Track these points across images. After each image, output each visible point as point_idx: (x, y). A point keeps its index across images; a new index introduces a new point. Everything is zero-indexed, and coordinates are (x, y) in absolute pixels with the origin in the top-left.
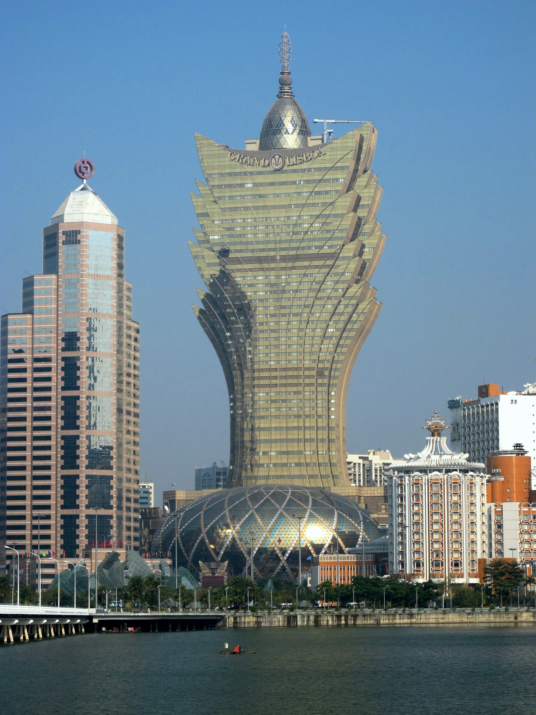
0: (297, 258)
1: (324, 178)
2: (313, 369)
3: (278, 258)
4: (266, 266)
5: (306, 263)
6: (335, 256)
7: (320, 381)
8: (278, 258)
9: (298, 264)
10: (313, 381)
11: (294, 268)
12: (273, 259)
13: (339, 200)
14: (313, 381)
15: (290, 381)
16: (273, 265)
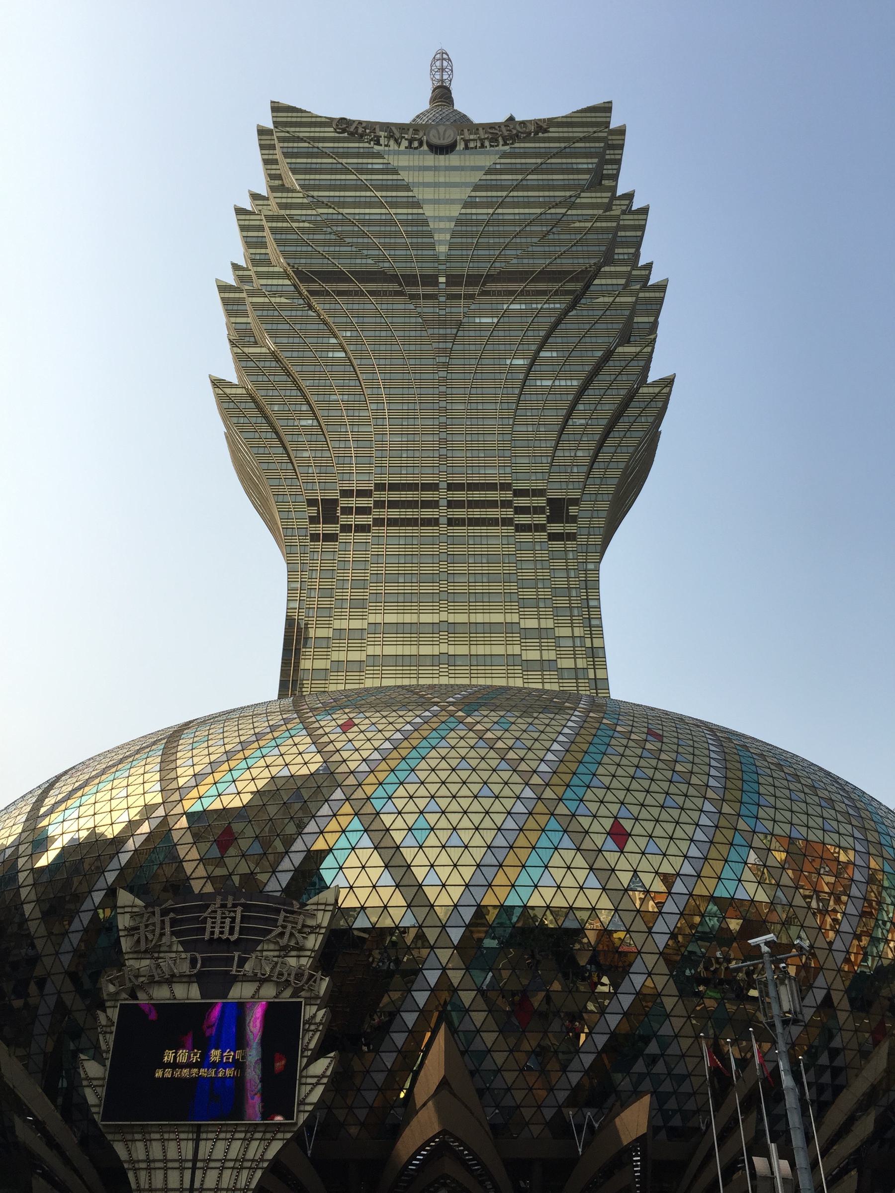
0: (490, 278)
1: (549, 161)
2: (540, 493)
3: (442, 280)
4: (412, 290)
5: (512, 286)
6: (587, 277)
7: (556, 528)
8: (442, 280)
9: (490, 287)
10: (541, 519)
11: (484, 293)
12: (430, 280)
13: (583, 195)
14: (541, 519)
15: (477, 513)
16: (429, 290)
